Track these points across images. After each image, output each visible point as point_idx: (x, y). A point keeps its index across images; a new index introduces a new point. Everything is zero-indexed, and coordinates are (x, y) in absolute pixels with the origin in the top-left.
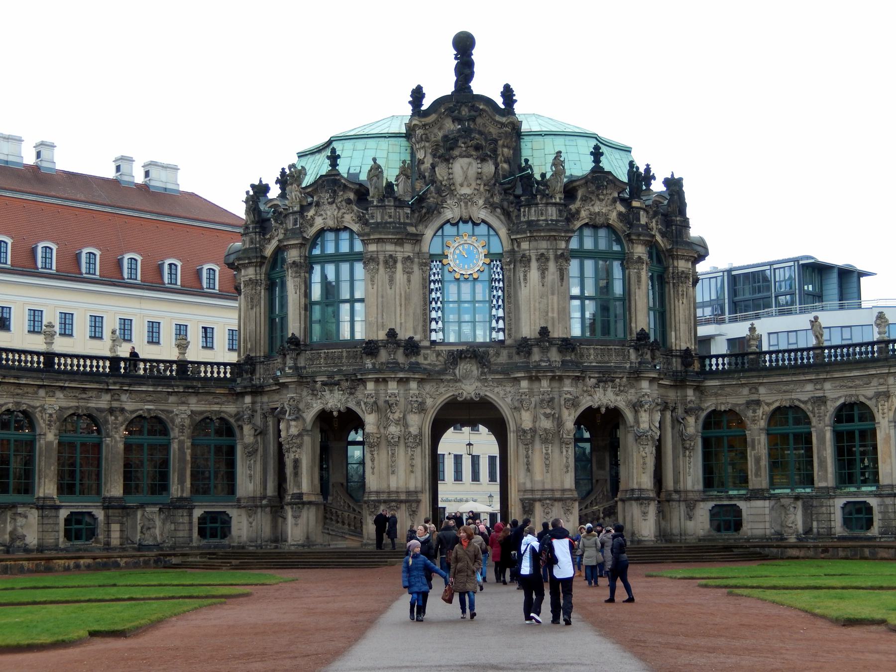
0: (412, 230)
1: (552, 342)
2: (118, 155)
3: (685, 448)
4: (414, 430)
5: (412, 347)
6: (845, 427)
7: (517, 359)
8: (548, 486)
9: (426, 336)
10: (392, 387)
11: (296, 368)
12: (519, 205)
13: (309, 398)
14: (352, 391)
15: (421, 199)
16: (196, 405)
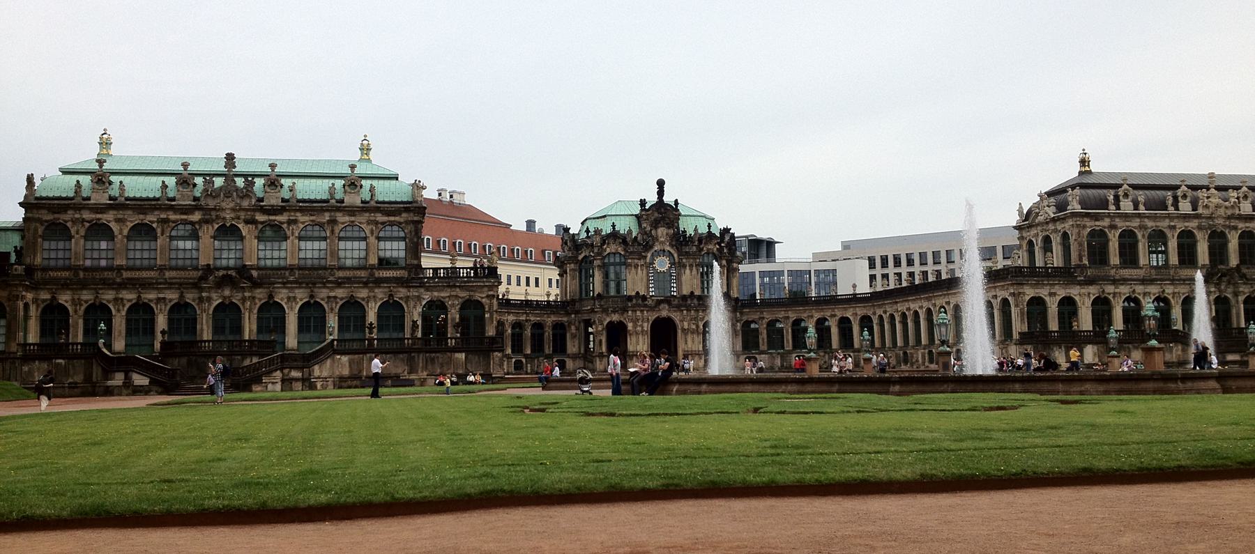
0: (643, 254)
1: (695, 296)
2: (439, 188)
3: (736, 335)
4: (646, 329)
5: (644, 298)
6: (795, 327)
7: (681, 302)
8: (694, 349)
9: (649, 294)
10: (638, 313)
11: (601, 306)
12: (682, 245)
13: (605, 317)
14: (622, 314)
15: (647, 243)
16: (553, 318)
